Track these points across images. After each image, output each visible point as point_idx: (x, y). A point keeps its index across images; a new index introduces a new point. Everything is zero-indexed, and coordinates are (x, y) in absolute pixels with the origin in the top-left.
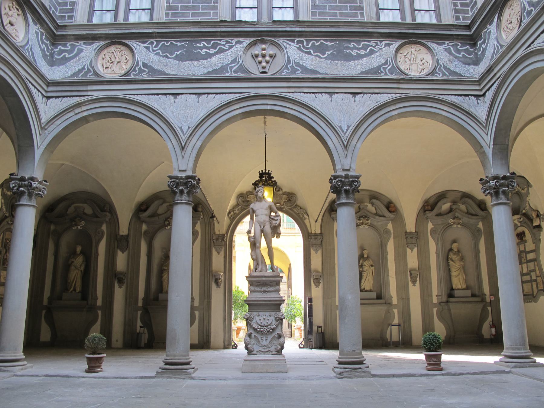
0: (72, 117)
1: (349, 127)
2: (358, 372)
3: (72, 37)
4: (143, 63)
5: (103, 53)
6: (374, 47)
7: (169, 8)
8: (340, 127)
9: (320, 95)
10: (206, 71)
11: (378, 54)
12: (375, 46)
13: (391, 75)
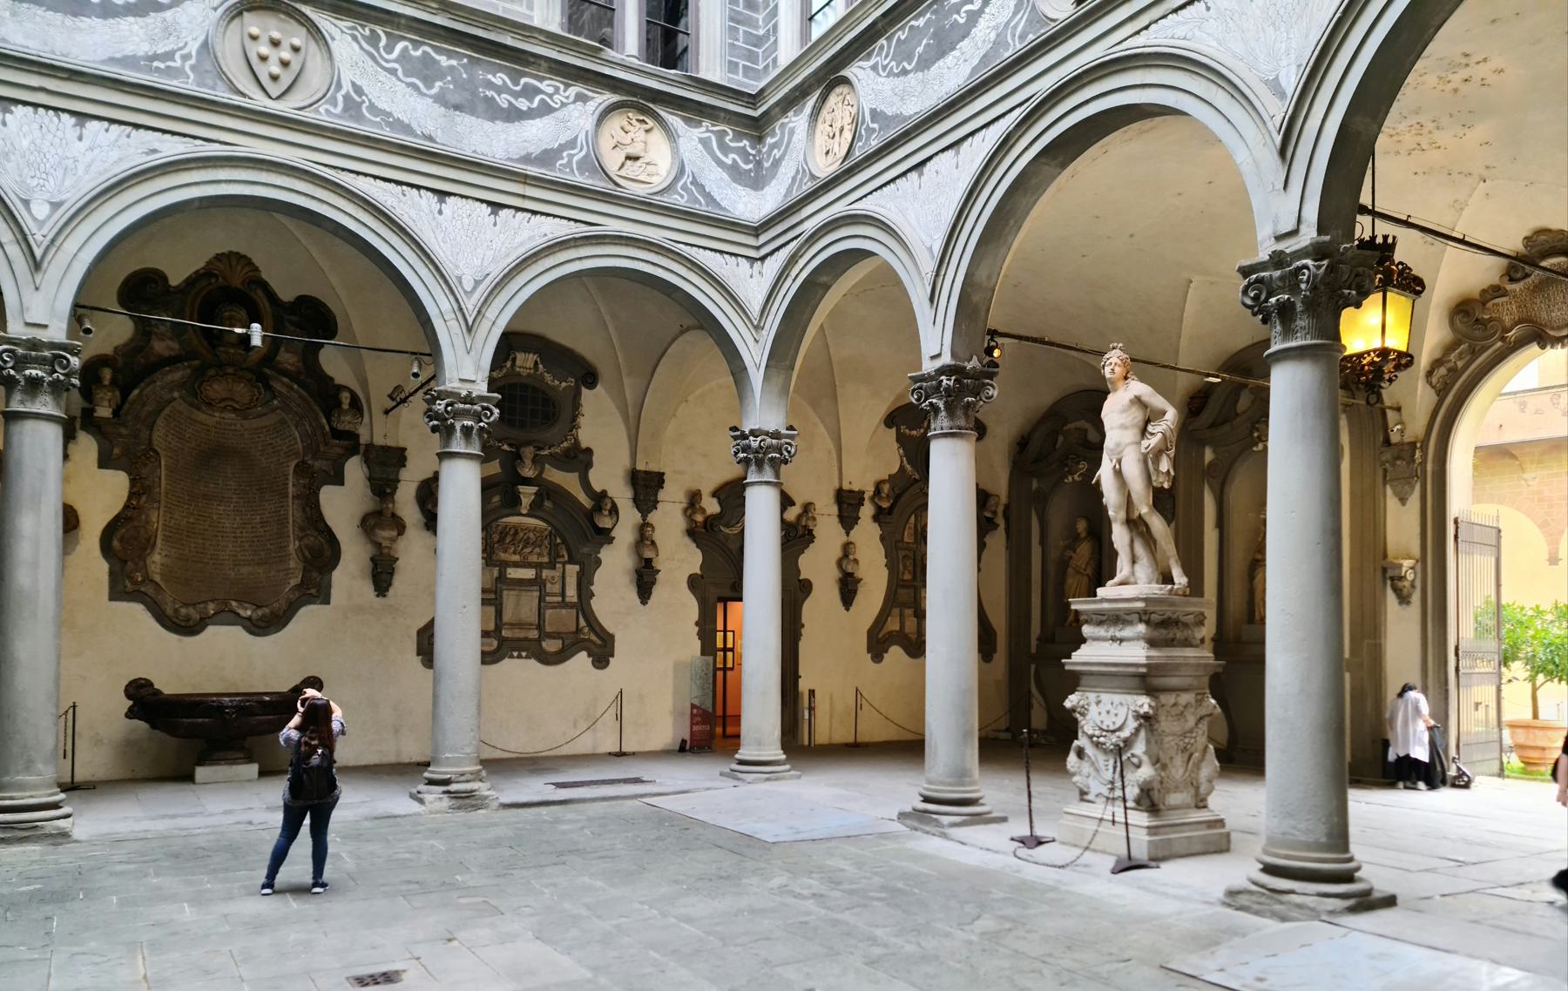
0: (791, 287)
2: (1281, 903)
3: (777, 109)
5: (820, 120)
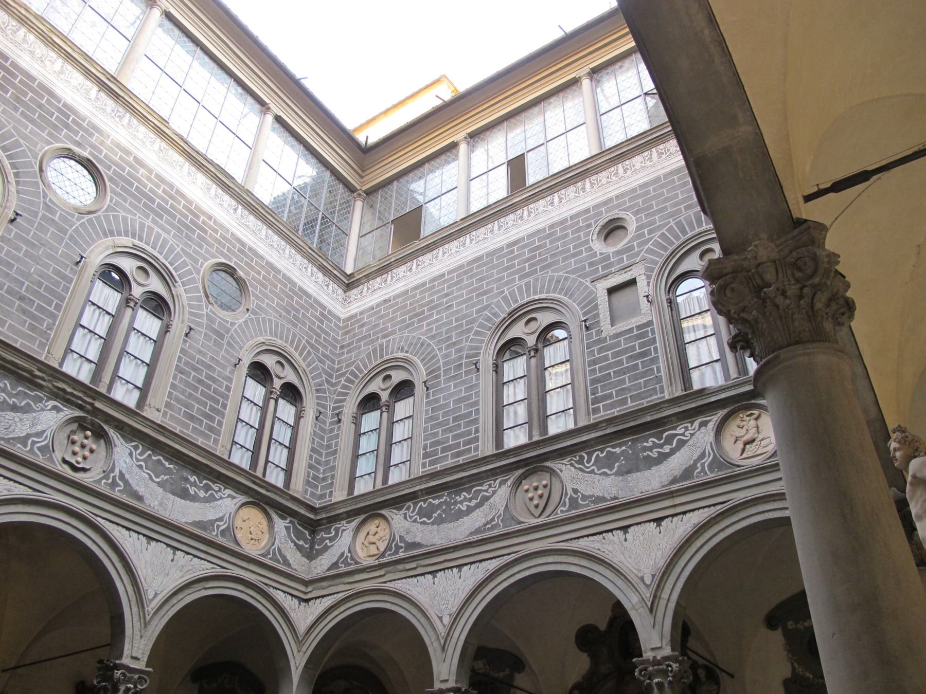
1: (653, 576)
4: (400, 537)
6: (683, 435)
7: (426, 455)
8: (642, 579)
9: (610, 534)
10: (467, 533)
11: (690, 443)
12: (684, 433)
13: (712, 475)
